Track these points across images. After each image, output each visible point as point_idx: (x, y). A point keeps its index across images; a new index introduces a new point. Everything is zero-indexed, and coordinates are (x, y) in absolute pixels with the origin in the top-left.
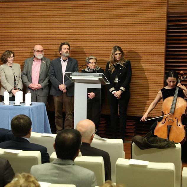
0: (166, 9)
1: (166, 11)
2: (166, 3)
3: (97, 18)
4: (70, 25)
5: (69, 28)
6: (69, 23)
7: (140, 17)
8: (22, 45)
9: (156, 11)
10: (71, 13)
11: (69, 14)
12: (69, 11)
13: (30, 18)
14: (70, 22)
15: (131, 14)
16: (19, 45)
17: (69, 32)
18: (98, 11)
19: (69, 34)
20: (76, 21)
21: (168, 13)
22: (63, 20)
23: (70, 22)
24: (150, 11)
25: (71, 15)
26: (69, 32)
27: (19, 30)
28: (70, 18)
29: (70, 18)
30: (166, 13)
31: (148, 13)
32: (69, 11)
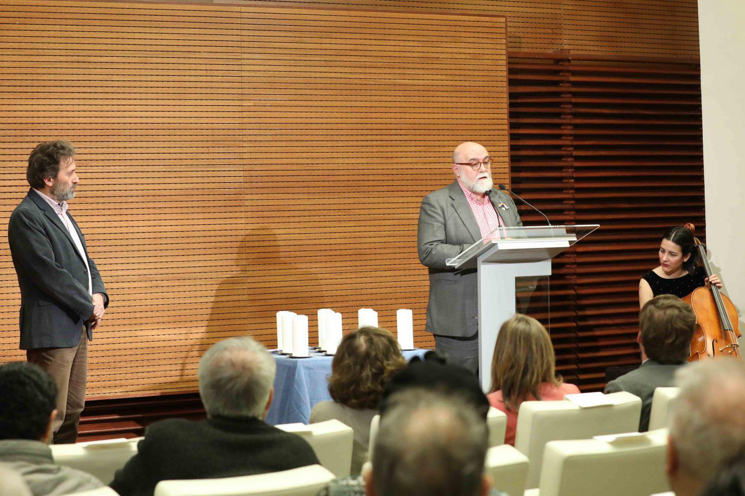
1: (504, 52)
14: (244, 74)
15: (420, 55)
23: (244, 74)
25: (246, 50)
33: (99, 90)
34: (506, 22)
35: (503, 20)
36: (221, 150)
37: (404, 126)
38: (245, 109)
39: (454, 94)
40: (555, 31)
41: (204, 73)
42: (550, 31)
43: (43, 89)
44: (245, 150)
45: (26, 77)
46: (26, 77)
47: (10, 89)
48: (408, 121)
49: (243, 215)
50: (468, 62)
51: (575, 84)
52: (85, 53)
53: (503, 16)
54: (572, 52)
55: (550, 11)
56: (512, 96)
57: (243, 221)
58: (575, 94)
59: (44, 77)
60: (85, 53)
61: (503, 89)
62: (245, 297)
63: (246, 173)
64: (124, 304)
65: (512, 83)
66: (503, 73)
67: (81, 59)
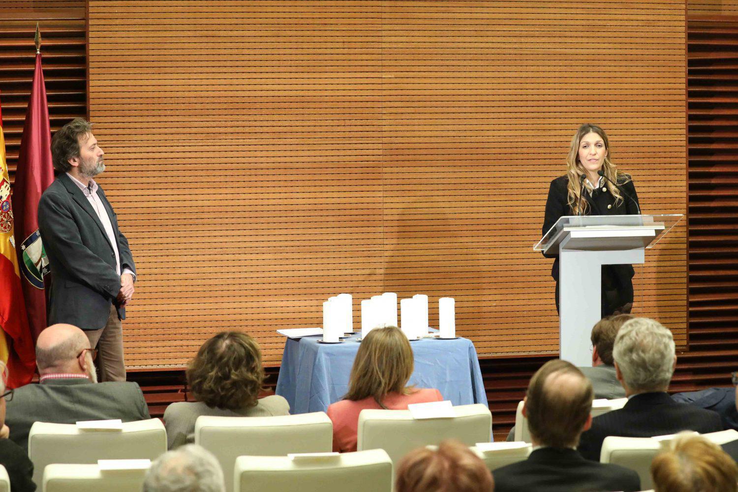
0: (683, 12)
1: (683, 18)
4: (384, 57)
5: (380, 69)
6: (380, 51)
8: (206, 130)
9: (656, 18)
10: (384, 15)
14: (384, 45)
15: (584, 23)
16: (194, 130)
17: (380, 81)
19: (379, 87)
21: (690, 25)
23: (384, 45)
25: (386, 21)
26: (380, 81)
28: (384, 33)
29: (384, 33)
30: (683, 24)
31: (635, 23)
33: (229, 63)
36: (359, 122)
37: (564, 97)
38: (384, 81)
39: (624, 63)
41: (341, 45)
43: (170, 64)
44: (384, 122)
45: (152, 52)
46: (152, 52)
47: (136, 64)
48: (568, 92)
49: (381, 188)
50: (642, 29)
52: (214, 27)
56: (690, 63)
57: (381, 194)
59: (171, 52)
60: (214, 27)
61: (681, 57)
63: (385, 146)
64: (252, 275)
65: (691, 49)
66: (681, 40)
67: (210, 33)
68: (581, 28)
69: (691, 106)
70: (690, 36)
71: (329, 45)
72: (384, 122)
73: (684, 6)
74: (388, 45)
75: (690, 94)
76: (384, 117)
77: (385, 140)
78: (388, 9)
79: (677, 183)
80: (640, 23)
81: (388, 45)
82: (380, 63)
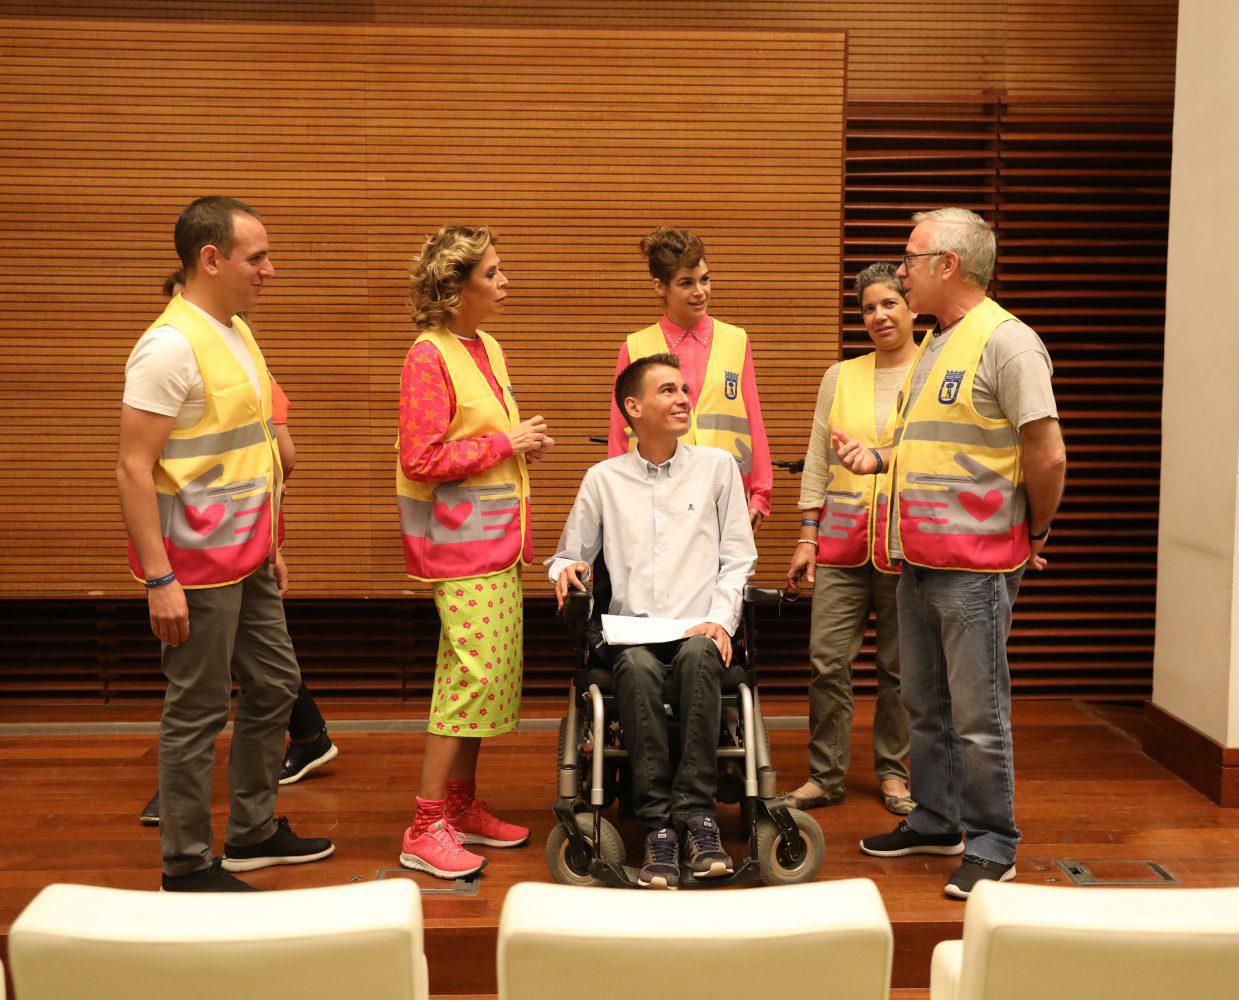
0: (842, 80)
2: (841, 56)
3: (508, 115)
4: (369, 149)
5: (363, 167)
6: (363, 140)
7: (721, 117)
10: (369, 86)
11: (362, 95)
12: (362, 76)
13: (144, 110)
14: (368, 131)
17: (363, 185)
18: (514, 79)
19: (363, 194)
20: (401, 131)
21: (850, 106)
22: (332, 122)
23: (368, 131)
24: (768, 90)
25: (371, 95)
26: (363, 185)
27: (83, 173)
28: (369, 113)
29: (369, 113)
32: (362, 76)
34: (846, 41)
35: (841, 36)
40: (989, 59)
41: (304, 131)
42: (979, 60)
44: (370, 247)
49: (365, 344)
51: (1011, 145)
53: (839, 30)
54: (1010, 93)
55: (979, 25)
56: (850, 166)
57: (365, 353)
58: (1010, 164)
62: (367, 466)
63: (372, 283)
68: (676, 108)
69: (849, 232)
70: (851, 125)
71: (285, 130)
72: (370, 247)
73: (841, 72)
74: (374, 131)
75: (849, 215)
76: (371, 239)
77: (372, 274)
78: (374, 77)
79: (825, 346)
80: (772, 100)
81: (374, 131)
82: (363, 158)
